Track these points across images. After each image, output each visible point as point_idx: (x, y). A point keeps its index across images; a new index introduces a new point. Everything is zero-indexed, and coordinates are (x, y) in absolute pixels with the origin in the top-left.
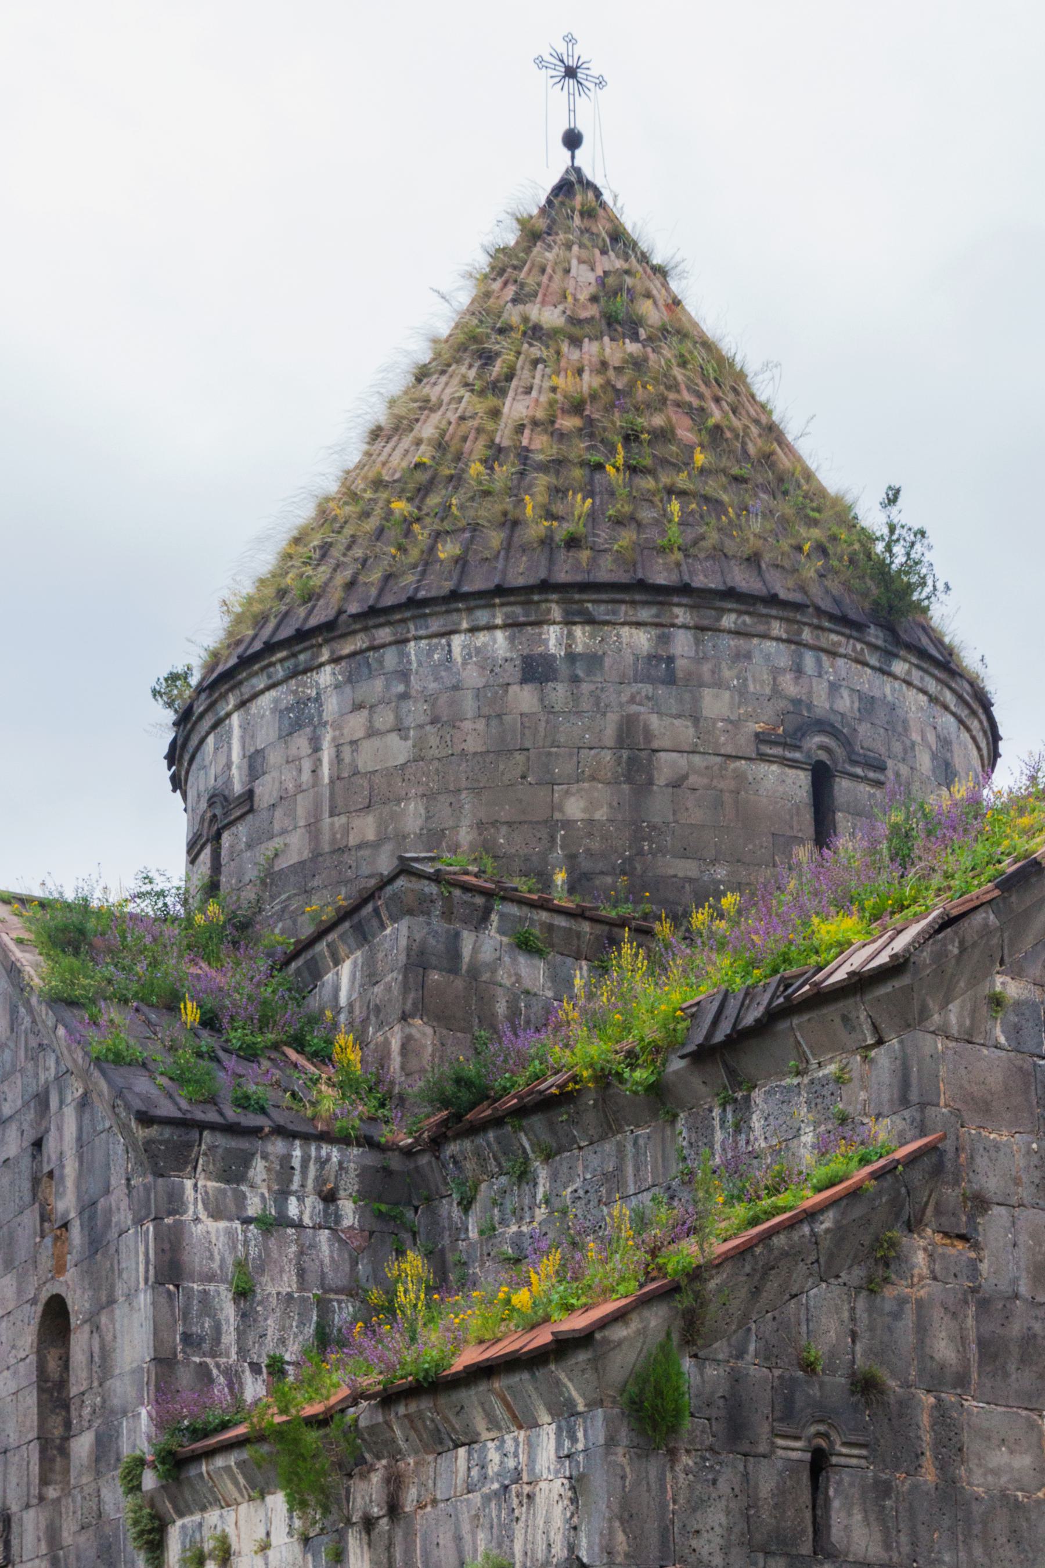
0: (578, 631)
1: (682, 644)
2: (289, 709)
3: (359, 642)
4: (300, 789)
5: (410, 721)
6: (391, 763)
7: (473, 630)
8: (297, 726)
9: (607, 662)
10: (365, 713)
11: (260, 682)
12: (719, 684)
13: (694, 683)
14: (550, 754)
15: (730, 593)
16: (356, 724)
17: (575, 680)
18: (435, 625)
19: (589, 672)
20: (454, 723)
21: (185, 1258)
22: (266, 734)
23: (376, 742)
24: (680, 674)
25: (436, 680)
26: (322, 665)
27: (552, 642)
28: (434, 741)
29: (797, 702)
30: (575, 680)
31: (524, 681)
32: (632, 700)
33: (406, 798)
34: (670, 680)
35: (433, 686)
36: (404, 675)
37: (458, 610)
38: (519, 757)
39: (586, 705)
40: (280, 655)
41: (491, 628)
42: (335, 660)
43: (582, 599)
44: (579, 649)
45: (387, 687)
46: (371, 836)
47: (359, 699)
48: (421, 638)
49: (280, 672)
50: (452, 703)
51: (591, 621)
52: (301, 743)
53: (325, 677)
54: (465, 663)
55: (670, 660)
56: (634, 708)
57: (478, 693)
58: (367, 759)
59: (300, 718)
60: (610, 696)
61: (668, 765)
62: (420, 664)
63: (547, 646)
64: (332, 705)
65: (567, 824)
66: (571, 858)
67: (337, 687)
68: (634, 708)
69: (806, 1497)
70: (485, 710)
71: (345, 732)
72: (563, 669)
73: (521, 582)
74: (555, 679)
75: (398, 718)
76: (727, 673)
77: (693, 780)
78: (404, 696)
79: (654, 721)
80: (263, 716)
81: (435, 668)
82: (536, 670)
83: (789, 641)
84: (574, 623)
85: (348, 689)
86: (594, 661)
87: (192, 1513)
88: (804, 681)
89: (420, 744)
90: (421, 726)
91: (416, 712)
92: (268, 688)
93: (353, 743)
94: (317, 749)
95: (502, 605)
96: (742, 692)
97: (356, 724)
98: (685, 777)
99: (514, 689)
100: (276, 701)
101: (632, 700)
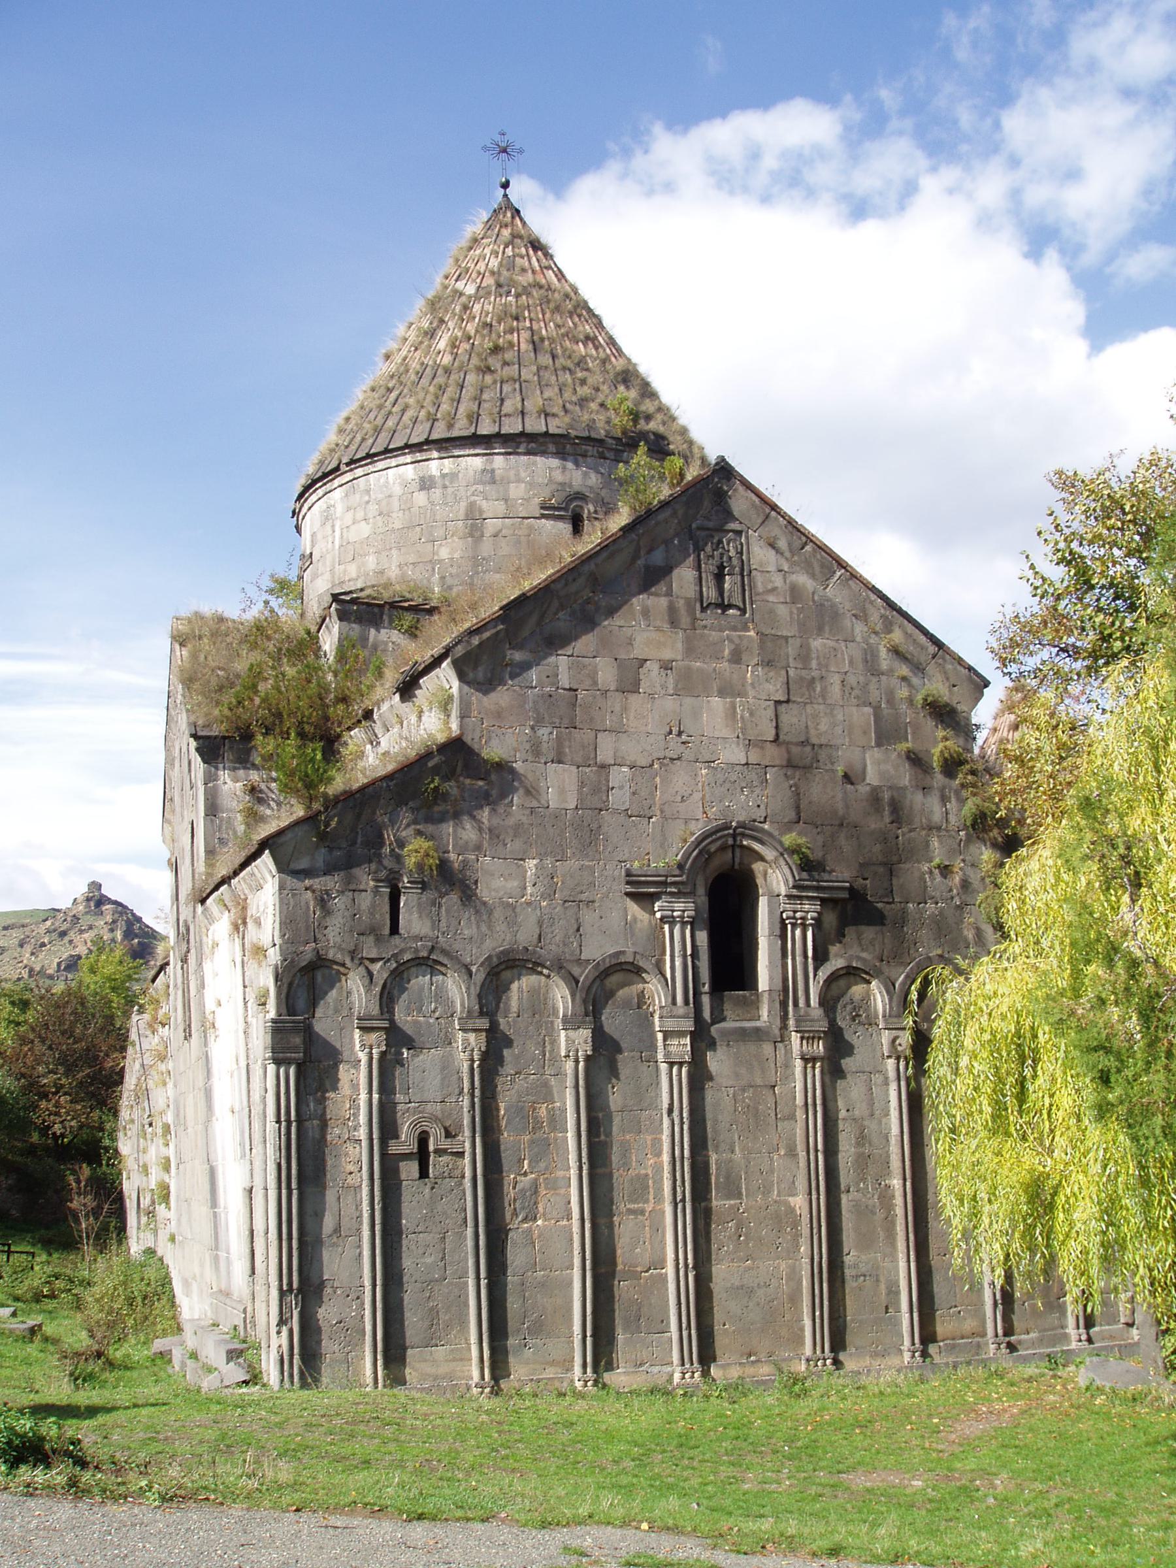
1: (499, 461)
8: (327, 519)
9: (460, 475)
11: (314, 498)
12: (519, 480)
13: (506, 481)
16: (349, 517)
17: (445, 487)
21: (219, 802)
22: (318, 524)
24: (497, 478)
29: (562, 484)
31: (421, 490)
33: (368, 554)
34: (493, 481)
35: (380, 496)
36: (368, 492)
38: (418, 529)
39: (450, 499)
43: (446, 445)
44: (446, 471)
46: (354, 575)
50: (388, 504)
53: (338, 494)
55: (493, 471)
56: (473, 498)
58: (353, 536)
59: (327, 518)
60: (462, 492)
61: (491, 525)
64: (340, 508)
65: (440, 561)
66: (443, 578)
68: (473, 498)
69: (387, 908)
72: (439, 482)
73: (416, 441)
76: (523, 474)
77: (504, 532)
79: (484, 505)
86: (453, 476)
88: (567, 473)
91: (373, 509)
97: (349, 517)
98: (500, 531)
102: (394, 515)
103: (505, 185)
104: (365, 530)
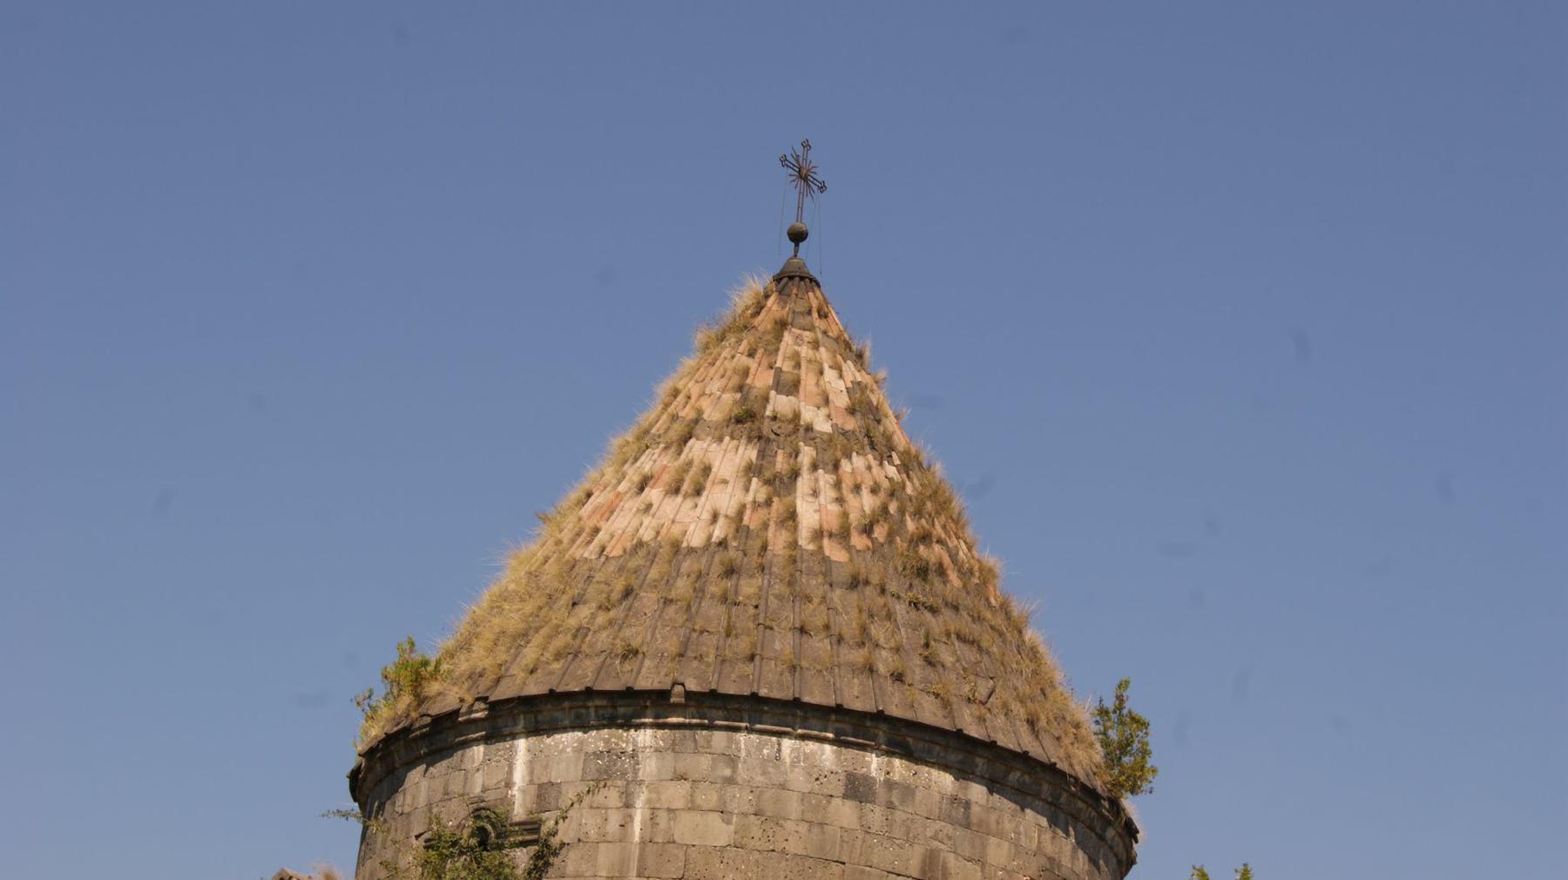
0: (897, 762)
2: (598, 755)
4: (603, 838)
5: (733, 806)
6: (710, 842)
9: (919, 795)
10: (687, 785)
12: (1000, 835)
14: (863, 872)
15: (1024, 757)
16: (676, 794)
19: (903, 802)
20: (778, 820)
23: (696, 817)
24: (974, 820)
25: (764, 773)
27: (874, 766)
28: (756, 832)
29: (1051, 860)
30: (890, 806)
31: (845, 796)
32: (935, 837)
34: (968, 826)
35: (760, 779)
36: (732, 760)
38: (836, 868)
40: (598, 702)
44: (896, 778)
45: (713, 767)
47: (681, 768)
52: (611, 797)
54: (793, 764)
55: (967, 805)
57: (804, 797)
58: (685, 828)
62: (749, 753)
63: (869, 767)
64: (649, 767)
70: (809, 816)
71: (663, 797)
74: (873, 802)
75: (722, 800)
78: (730, 781)
79: (951, 858)
80: (562, 751)
81: (764, 762)
82: (857, 789)
83: (1051, 804)
85: (670, 756)
86: (908, 791)
89: (742, 831)
90: (744, 814)
91: (740, 800)
93: (669, 810)
94: (628, 805)
96: (1016, 844)
99: (837, 802)
100: (581, 742)
101: (935, 837)
102: (790, 826)
104: (719, 832)
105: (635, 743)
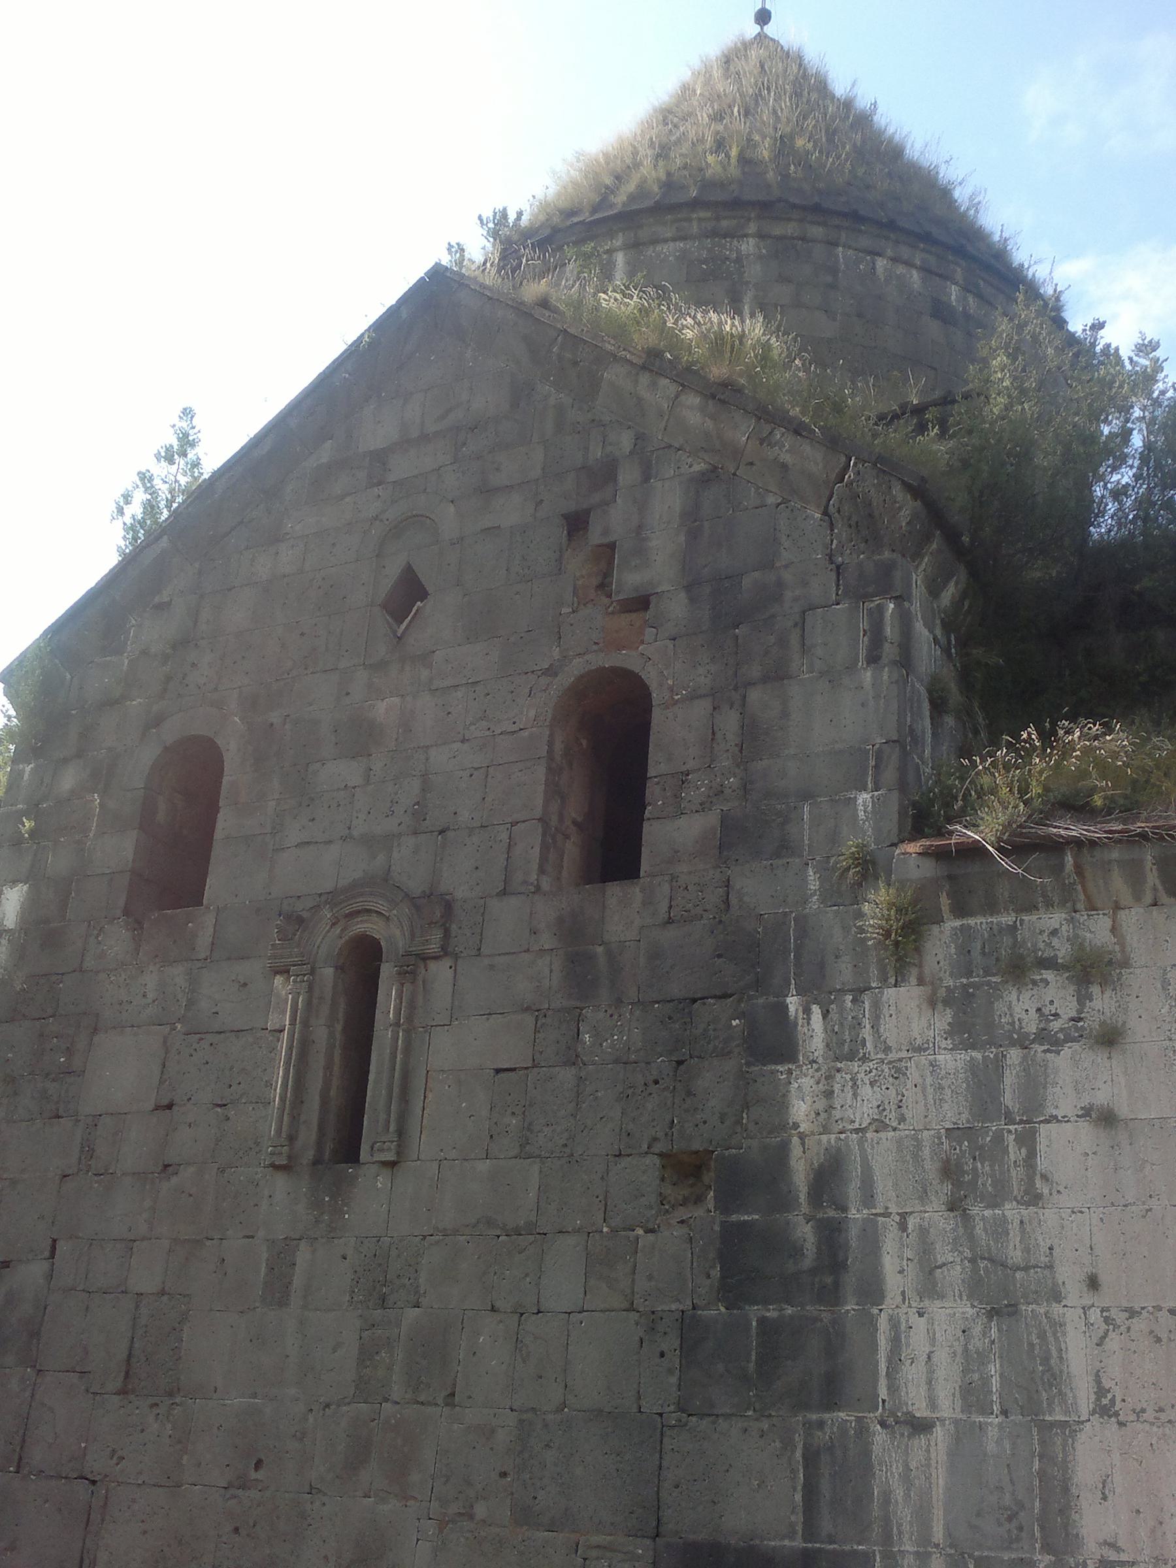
3: (791, 229)
7: (895, 260)
18: (865, 242)
26: (746, 236)
36: (834, 271)
37: (887, 238)
40: (702, 214)
41: (909, 264)
42: (761, 236)
48: (850, 247)
49: (695, 229)
51: (979, 296)
53: (748, 246)
64: (754, 271)
67: (760, 257)
78: (833, 286)
84: (969, 291)
87: (991, 907)
92: (674, 240)
95: (923, 250)
103: (763, 17)
105: (738, 251)
